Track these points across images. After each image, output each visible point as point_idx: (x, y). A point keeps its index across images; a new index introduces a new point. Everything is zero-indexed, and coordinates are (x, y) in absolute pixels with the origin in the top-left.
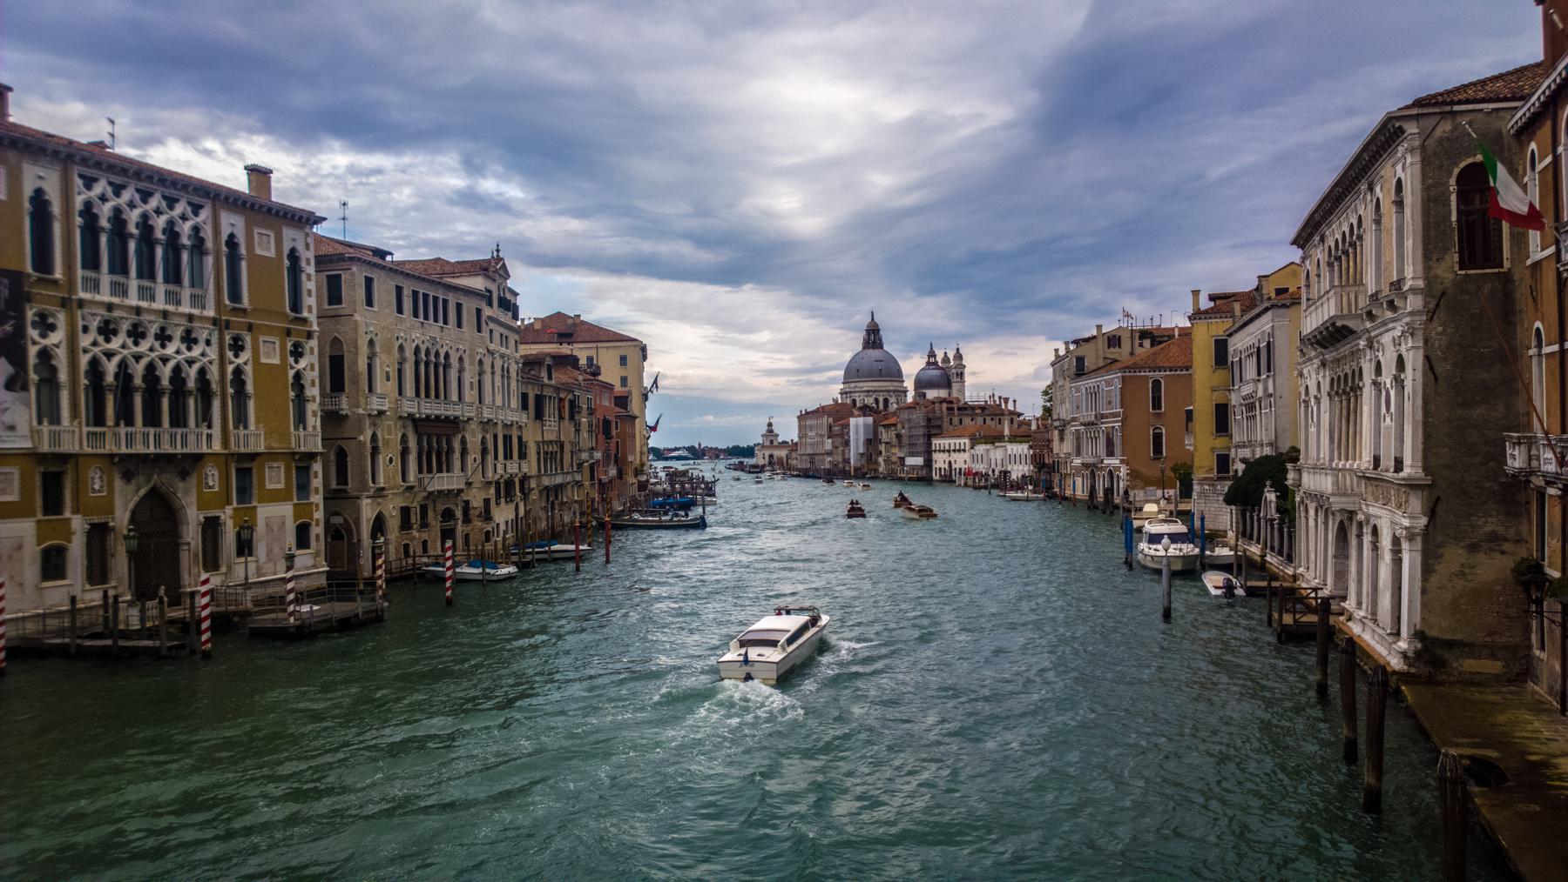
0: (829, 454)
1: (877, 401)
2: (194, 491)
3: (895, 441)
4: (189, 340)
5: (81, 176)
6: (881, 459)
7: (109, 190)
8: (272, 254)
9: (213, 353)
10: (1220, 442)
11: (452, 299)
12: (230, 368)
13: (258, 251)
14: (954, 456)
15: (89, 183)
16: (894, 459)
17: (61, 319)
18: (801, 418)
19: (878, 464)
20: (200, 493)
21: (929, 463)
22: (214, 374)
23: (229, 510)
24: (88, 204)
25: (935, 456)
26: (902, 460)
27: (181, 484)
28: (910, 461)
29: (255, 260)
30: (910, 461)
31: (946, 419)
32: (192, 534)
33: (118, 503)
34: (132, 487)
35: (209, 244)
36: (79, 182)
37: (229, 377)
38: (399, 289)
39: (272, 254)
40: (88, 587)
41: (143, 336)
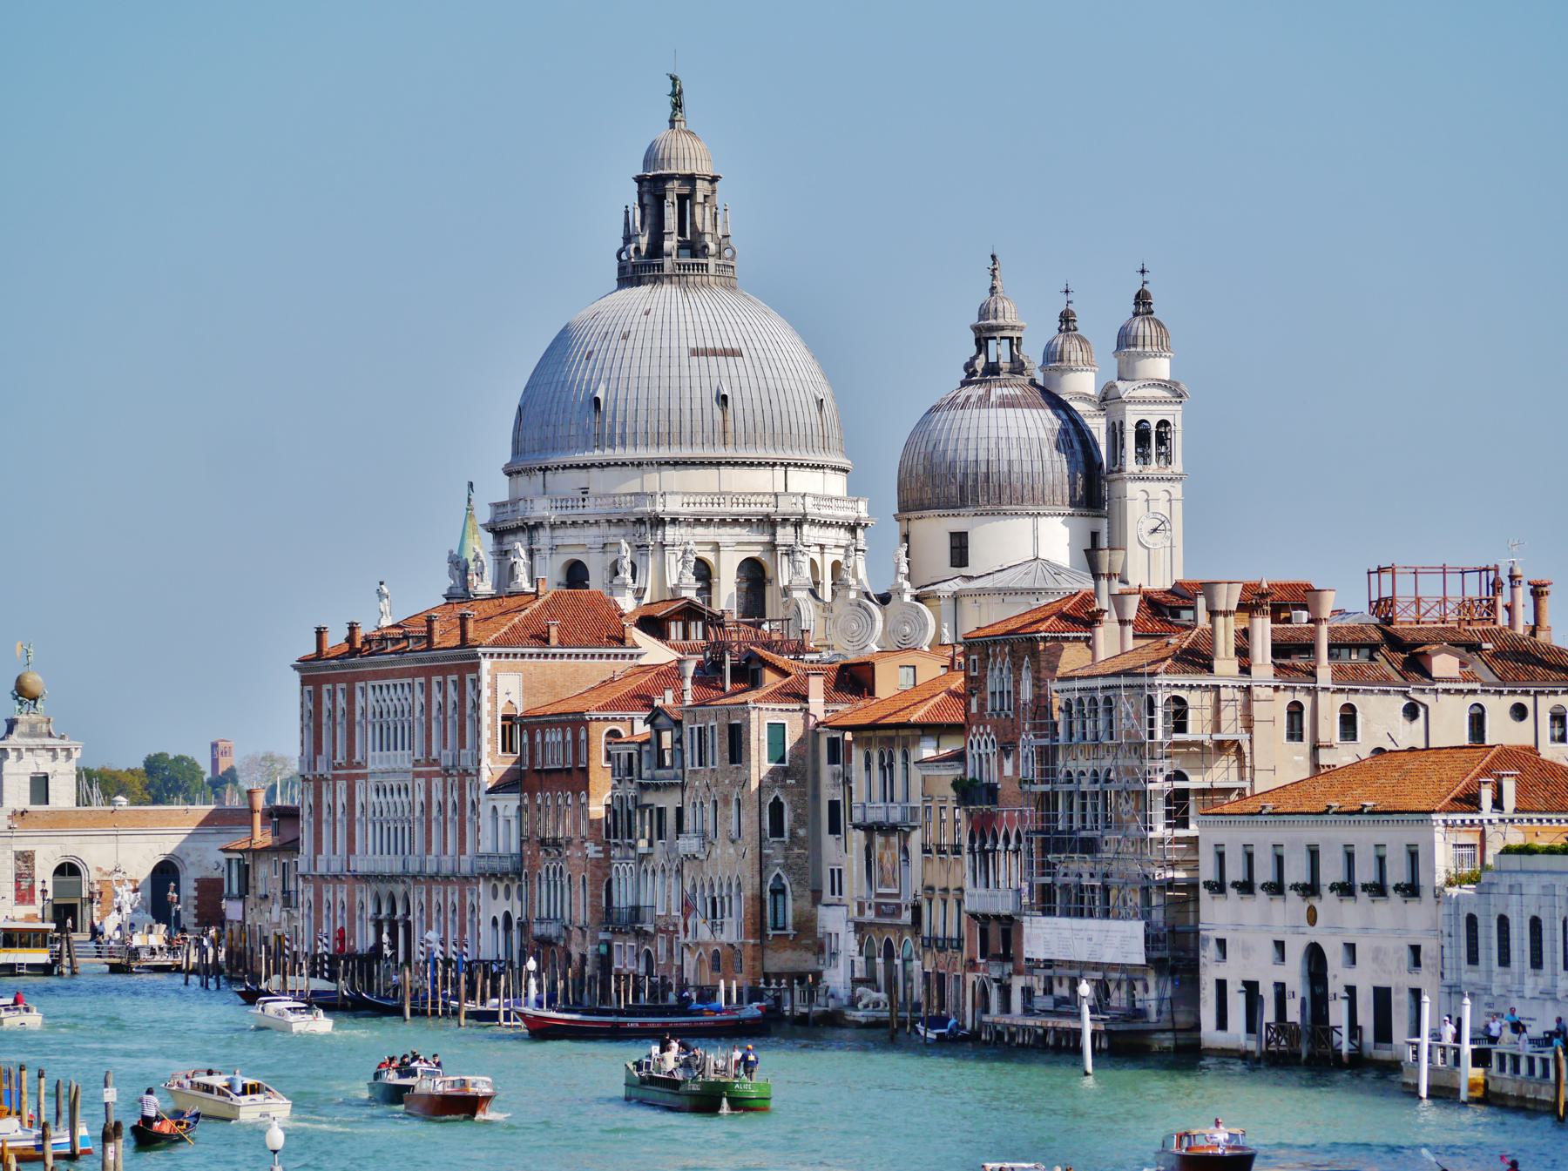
0: (511, 874)
1: (704, 572)
3: (954, 822)
6: (835, 921)
14: (1341, 921)
16: (941, 921)
18: (316, 672)
19: (821, 948)
21: (1175, 953)
25: (1215, 915)
26: (1000, 936)
28: (1046, 937)
30: (1046, 937)
31: (1272, 708)
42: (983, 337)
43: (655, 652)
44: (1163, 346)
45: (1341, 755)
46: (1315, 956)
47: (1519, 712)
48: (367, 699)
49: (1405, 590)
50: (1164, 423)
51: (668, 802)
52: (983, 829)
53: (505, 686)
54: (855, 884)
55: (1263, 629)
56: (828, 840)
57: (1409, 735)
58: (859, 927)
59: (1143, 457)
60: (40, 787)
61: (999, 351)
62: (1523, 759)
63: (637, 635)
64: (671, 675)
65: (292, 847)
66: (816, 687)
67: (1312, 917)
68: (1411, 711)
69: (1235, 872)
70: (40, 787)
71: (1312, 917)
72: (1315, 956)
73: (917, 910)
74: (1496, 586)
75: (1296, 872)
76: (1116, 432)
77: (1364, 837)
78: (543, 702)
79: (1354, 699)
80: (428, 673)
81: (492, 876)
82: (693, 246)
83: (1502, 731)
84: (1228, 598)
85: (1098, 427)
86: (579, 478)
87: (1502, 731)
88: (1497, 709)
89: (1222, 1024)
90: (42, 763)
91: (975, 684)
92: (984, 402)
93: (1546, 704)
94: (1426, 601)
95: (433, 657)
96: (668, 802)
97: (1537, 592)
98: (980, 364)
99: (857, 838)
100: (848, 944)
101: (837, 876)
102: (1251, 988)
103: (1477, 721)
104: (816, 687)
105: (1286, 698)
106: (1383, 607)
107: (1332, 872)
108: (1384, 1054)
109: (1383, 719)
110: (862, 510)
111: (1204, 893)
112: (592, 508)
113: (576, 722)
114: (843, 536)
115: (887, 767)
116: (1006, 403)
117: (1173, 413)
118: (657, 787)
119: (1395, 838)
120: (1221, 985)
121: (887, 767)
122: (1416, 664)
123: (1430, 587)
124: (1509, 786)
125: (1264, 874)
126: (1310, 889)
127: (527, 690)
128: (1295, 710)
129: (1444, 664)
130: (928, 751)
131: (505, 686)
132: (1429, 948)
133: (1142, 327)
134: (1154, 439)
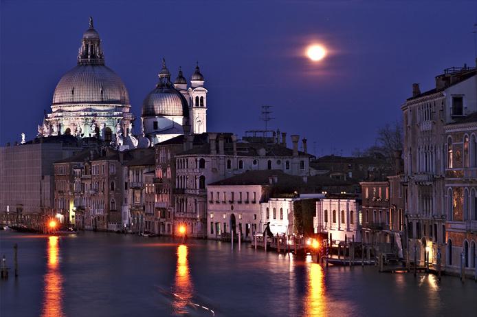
47: (279, 162)
50: (202, 97)
55: (221, 143)
58: (131, 211)
67: (232, 208)
68: (255, 162)
69: (215, 199)
71: (232, 208)
73: (144, 207)
83: (274, 166)
87: (274, 166)
88: (274, 161)
89: (212, 232)
93: (285, 160)
100: (129, 215)
103: (270, 163)
107: (237, 198)
108: (248, 239)
111: (208, 202)
115: (138, 174)
118: (85, 179)
120: (212, 223)
121: (138, 174)
126: (232, 202)
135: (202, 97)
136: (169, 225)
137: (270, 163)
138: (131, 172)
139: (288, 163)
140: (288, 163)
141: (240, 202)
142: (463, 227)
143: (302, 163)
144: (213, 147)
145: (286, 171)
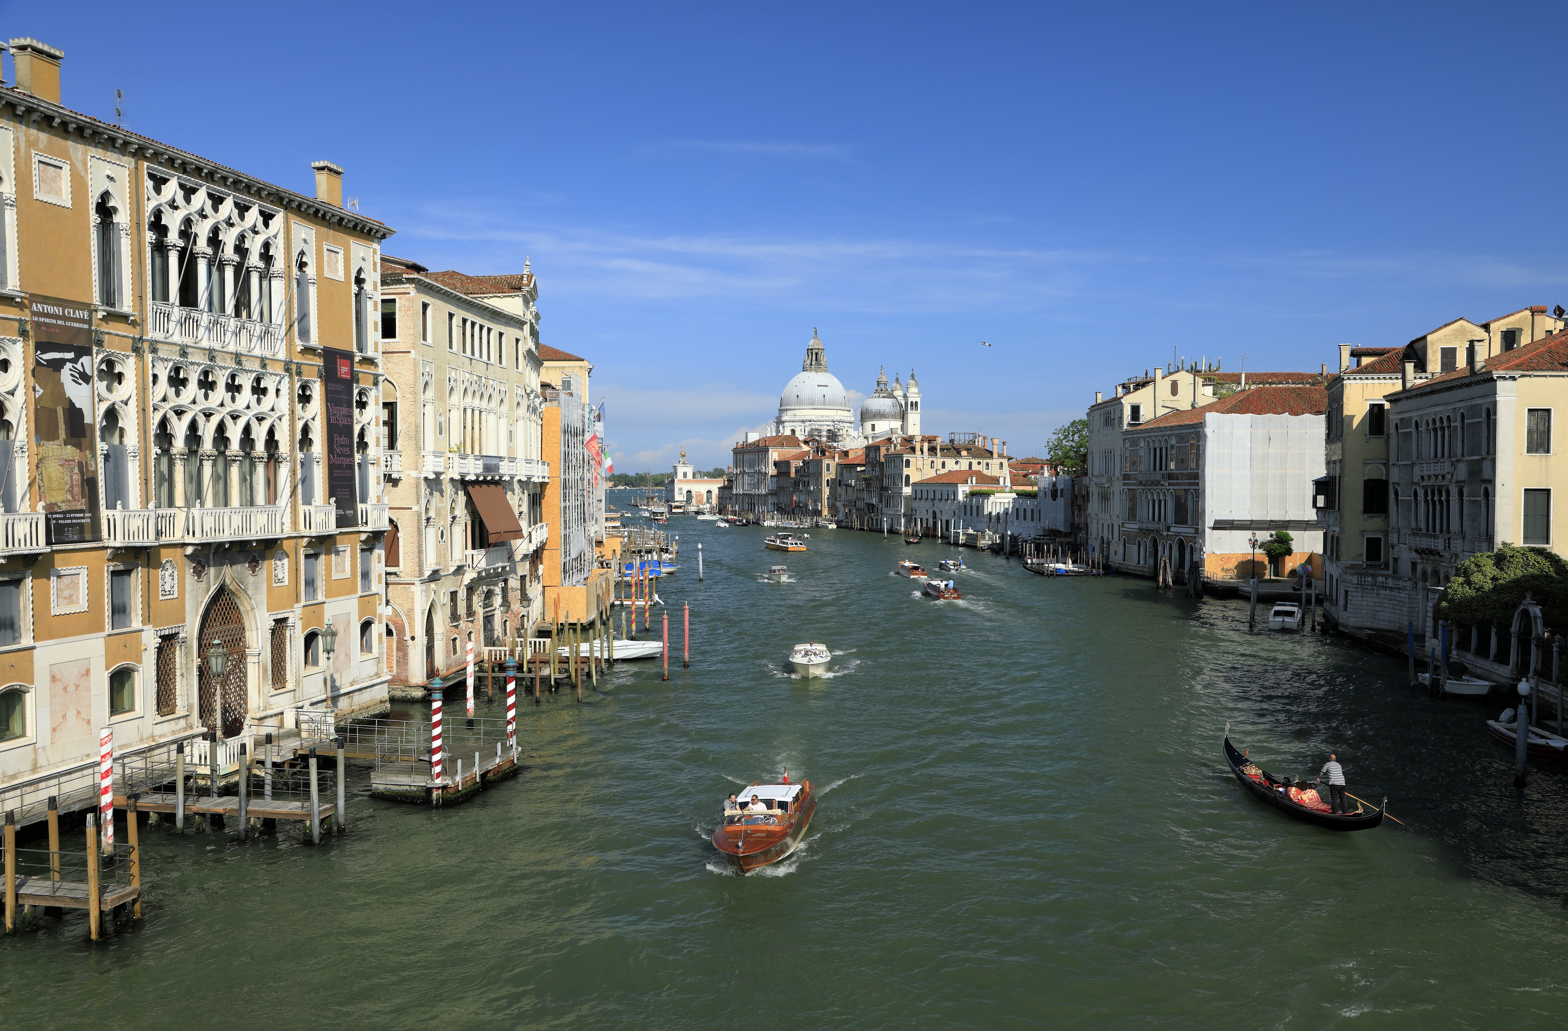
2: (264, 587)
4: (259, 391)
5: (151, 176)
7: (180, 194)
8: (340, 275)
9: (284, 404)
10: (1374, 524)
11: (496, 328)
12: (300, 425)
13: (327, 274)
15: (159, 182)
17: (128, 367)
20: (270, 589)
22: (282, 436)
23: (298, 608)
24: (158, 214)
27: (251, 579)
29: (324, 282)
32: (257, 639)
33: (189, 606)
34: (203, 585)
35: (279, 264)
36: (150, 184)
37: (299, 436)
38: (451, 316)
39: (340, 275)
40: (159, 719)
41: (184, 382)
42: (878, 383)
43: (805, 448)
44: (917, 385)
45: (942, 471)
46: (934, 512)
47: (979, 463)
48: (746, 457)
49: (957, 438)
50: (916, 402)
51: (806, 479)
52: (868, 485)
53: (774, 455)
54: (843, 497)
55: (926, 446)
56: (839, 488)
57: (956, 468)
59: (912, 409)
60: (685, 475)
61: (882, 386)
62: (978, 474)
63: (802, 445)
64: (808, 453)
65: (731, 488)
66: (837, 456)
68: (957, 463)
70: (685, 475)
72: (934, 512)
74: (975, 437)
75: (931, 496)
76: (906, 404)
77: (945, 489)
78: (782, 458)
79: (945, 460)
80: (759, 452)
81: (771, 494)
82: (818, 363)
83: (975, 467)
84: (919, 439)
85: (903, 403)
86: (794, 412)
87: (975, 467)
88: (975, 462)
90: (685, 469)
91: (867, 456)
92: (879, 397)
93: (985, 461)
94: (961, 439)
95: (760, 450)
96: (806, 479)
97: (985, 438)
98: (879, 389)
99: (844, 487)
101: (840, 495)
102: (921, 520)
104: (837, 456)
105: (931, 459)
106: (952, 441)
107: (938, 496)
109: (951, 464)
110: (853, 419)
112: (797, 418)
113: (787, 463)
114: (849, 425)
116: (883, 397)
117: (919, 400)
119: (951, 489)
122: (959, 453)
123: (962, 437)
124: (974, 479)
125: (925, 496)
127: (779, 456)
128: (932, 462)
129: (964, 453)
130: (859, 469)
131: (774, 455)
132: (957, 512)
133: (912, 382)
134: (914, 405)
135: (916, 402)
136: (877, 520)
137: (970, 464)
138: (844, 470)
139: (987, 464)
140: (987, 464)
141: (941, 500)
142: (1137, 526)
143: (1001, 464)
144: (918, 448)
145: (985, 472)
